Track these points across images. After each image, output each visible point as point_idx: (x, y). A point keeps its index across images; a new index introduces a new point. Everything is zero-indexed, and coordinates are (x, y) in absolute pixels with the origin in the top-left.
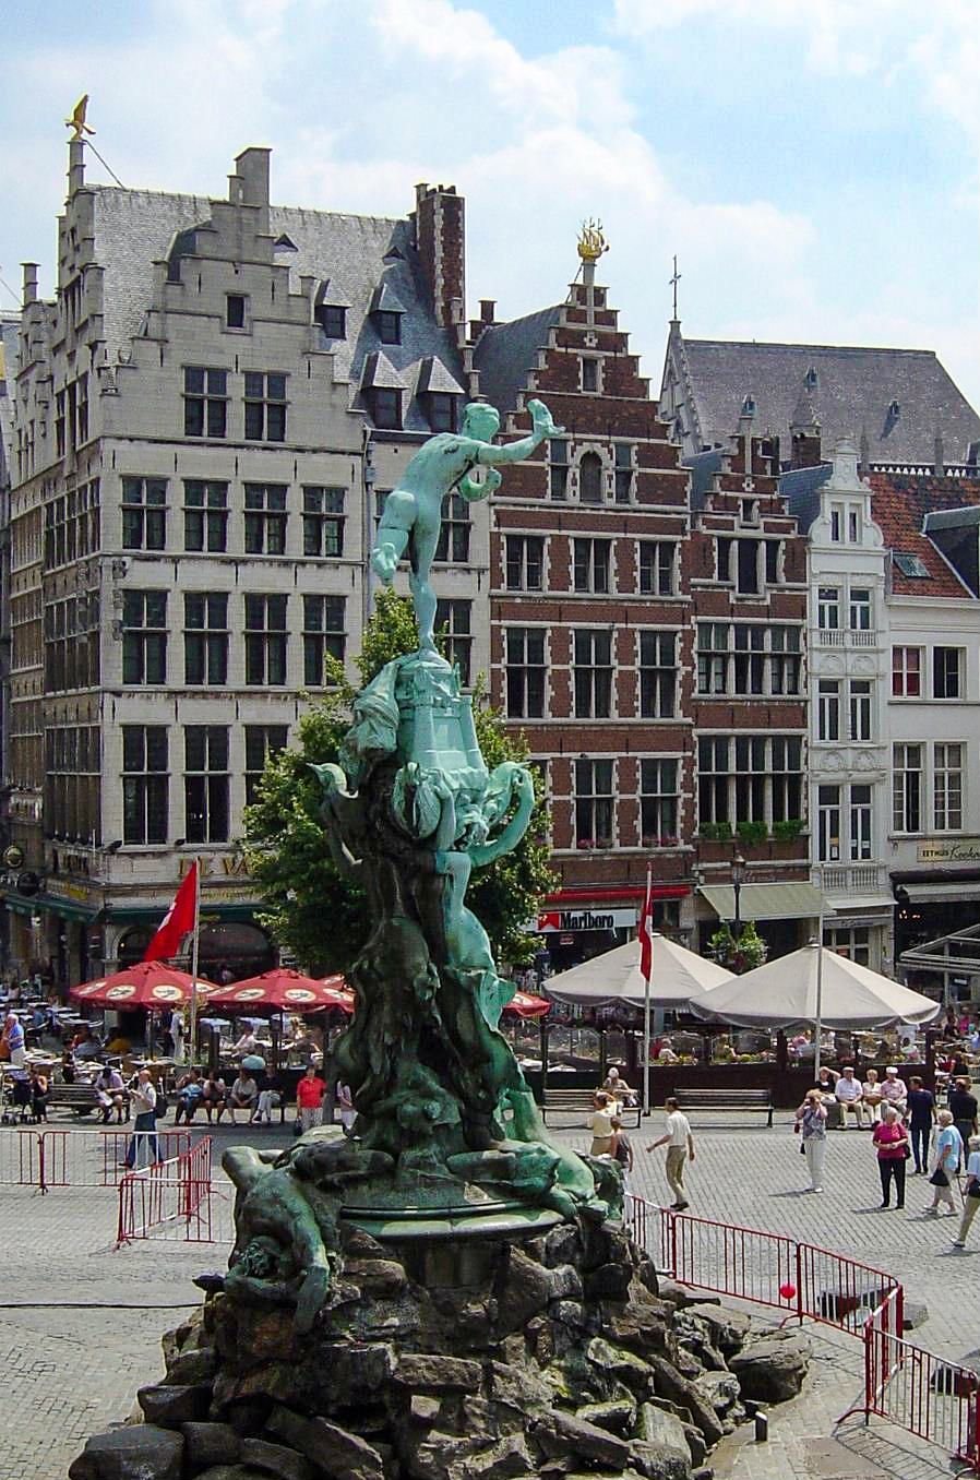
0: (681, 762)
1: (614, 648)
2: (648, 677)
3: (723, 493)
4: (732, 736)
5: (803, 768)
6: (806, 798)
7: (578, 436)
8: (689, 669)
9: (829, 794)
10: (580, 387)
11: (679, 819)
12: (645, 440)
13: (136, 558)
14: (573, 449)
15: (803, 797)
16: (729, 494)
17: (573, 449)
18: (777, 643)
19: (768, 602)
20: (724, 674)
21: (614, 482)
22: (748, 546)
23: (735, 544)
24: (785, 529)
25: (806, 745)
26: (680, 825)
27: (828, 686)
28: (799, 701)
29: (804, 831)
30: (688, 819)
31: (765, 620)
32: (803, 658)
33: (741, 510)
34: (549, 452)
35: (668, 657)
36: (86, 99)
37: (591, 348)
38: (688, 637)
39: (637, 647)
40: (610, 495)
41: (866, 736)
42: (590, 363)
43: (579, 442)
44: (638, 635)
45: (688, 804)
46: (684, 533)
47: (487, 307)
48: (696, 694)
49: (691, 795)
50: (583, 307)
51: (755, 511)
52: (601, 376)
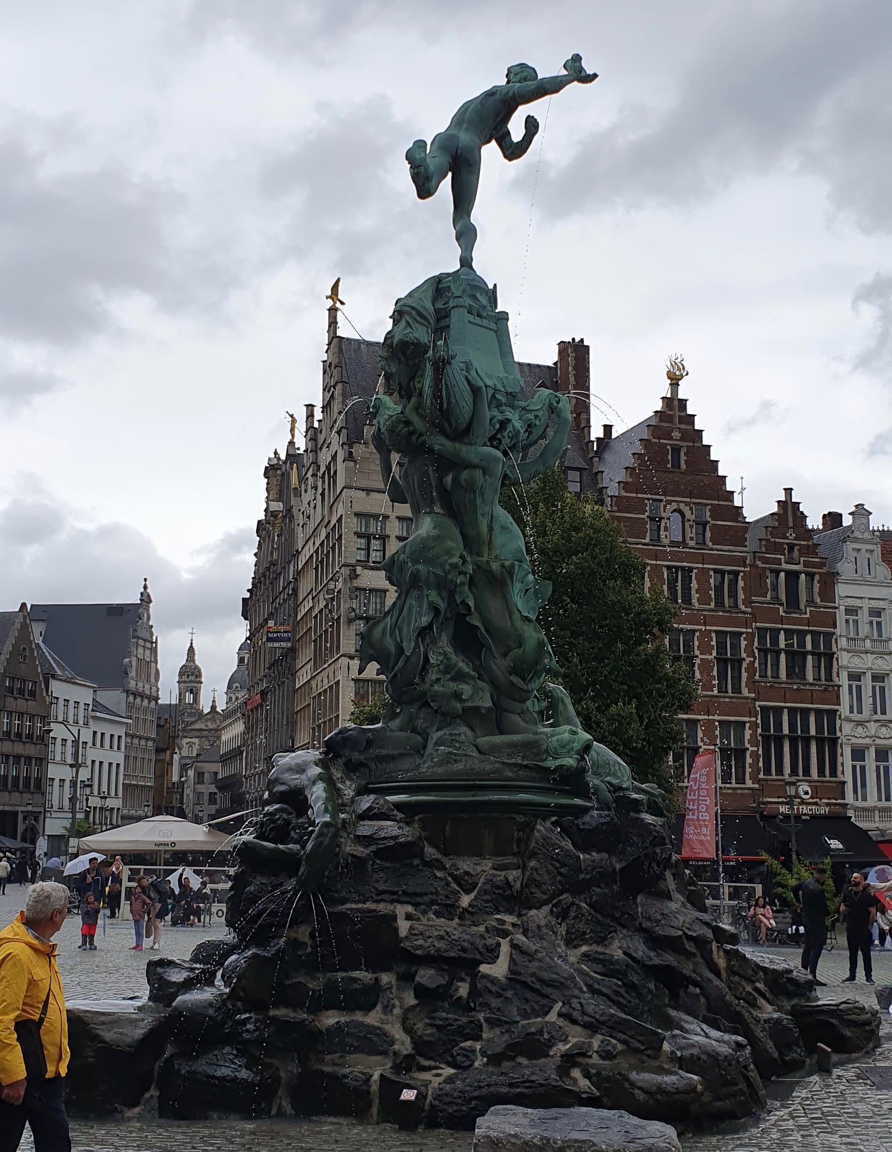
0: (748, 725)
1: (696, 643)
2: (722, 661)
3: (773, 540)
4: (785, 707)
5: (838, 734)
6: (842, 755)
7: (668, 498)
8: (752, 659)
9: (858, 754)
10: (669, 466)
11: (747, 766)
12: (716, 502)
13: (365, 567)
14: (665, 507)
15: (839, 754)
16: (777, 540)
17: (665, 507)
18: (815, 643)
19: (808, 615)
20: (776, 665)
21: (694, 530)
22: (792, 576)
23: (782, 574)
24: (821, 565)
25: (840, 718)
26: (748, 770)
27: (855, 677)
28: (833, 686)
29: (841, 778)
30: (753, 766)
31: (807, 628)
32: (835, 656)
33: (786, 551)
34: (647, 508)
35: (736, 647)
36: (338, 280)
37: (676, 440)
38: (750, 638)
39: (714, 643)
40: (692, 539)
41: (884, 712)
42: (676, 450)
43: (669, 502)
44: (713, 635)
45: (755, 755)
46: (745, 566)
47: (608, 429)
48: (757, 677)
49: (756, 749)
50: (671, 413)
51: (796, 553)
52: (683, 458)
